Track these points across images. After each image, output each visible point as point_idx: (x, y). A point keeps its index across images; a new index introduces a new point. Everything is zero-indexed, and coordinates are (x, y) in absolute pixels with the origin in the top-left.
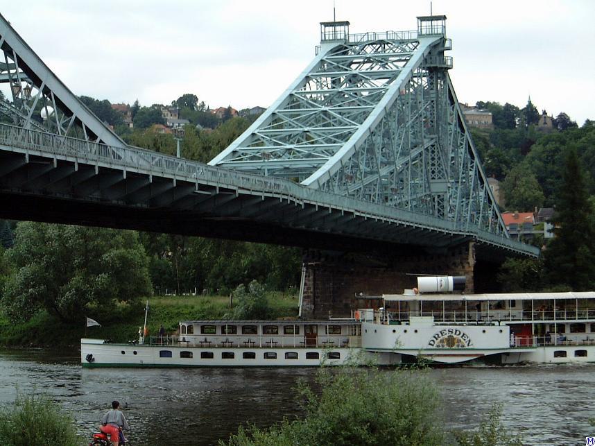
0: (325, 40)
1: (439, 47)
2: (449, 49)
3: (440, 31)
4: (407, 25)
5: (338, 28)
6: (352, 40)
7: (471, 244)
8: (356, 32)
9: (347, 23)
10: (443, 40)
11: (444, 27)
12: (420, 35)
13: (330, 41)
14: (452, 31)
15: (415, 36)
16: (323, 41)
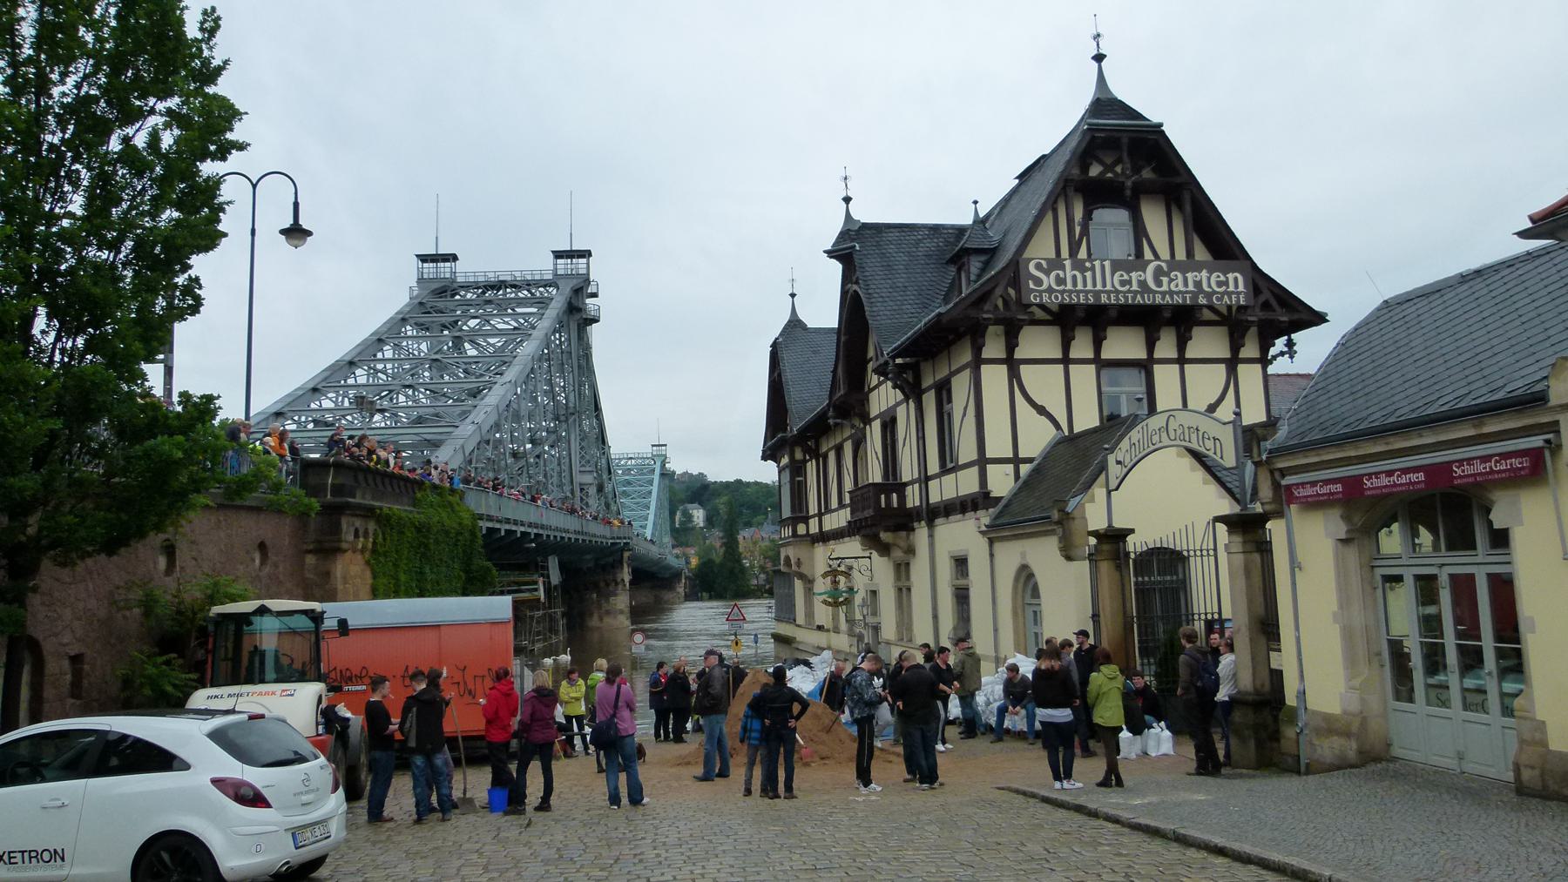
0: (423, 278)
1: (581, 289)
2: (595, 295)
3: (583, 271)
4: (543, 265)
7: (626, 554)
8: (469, 267)
9: (454, 258)
11: (588, 264)
12: (556, 275)
14: (599, 271)
16: (421, 280)
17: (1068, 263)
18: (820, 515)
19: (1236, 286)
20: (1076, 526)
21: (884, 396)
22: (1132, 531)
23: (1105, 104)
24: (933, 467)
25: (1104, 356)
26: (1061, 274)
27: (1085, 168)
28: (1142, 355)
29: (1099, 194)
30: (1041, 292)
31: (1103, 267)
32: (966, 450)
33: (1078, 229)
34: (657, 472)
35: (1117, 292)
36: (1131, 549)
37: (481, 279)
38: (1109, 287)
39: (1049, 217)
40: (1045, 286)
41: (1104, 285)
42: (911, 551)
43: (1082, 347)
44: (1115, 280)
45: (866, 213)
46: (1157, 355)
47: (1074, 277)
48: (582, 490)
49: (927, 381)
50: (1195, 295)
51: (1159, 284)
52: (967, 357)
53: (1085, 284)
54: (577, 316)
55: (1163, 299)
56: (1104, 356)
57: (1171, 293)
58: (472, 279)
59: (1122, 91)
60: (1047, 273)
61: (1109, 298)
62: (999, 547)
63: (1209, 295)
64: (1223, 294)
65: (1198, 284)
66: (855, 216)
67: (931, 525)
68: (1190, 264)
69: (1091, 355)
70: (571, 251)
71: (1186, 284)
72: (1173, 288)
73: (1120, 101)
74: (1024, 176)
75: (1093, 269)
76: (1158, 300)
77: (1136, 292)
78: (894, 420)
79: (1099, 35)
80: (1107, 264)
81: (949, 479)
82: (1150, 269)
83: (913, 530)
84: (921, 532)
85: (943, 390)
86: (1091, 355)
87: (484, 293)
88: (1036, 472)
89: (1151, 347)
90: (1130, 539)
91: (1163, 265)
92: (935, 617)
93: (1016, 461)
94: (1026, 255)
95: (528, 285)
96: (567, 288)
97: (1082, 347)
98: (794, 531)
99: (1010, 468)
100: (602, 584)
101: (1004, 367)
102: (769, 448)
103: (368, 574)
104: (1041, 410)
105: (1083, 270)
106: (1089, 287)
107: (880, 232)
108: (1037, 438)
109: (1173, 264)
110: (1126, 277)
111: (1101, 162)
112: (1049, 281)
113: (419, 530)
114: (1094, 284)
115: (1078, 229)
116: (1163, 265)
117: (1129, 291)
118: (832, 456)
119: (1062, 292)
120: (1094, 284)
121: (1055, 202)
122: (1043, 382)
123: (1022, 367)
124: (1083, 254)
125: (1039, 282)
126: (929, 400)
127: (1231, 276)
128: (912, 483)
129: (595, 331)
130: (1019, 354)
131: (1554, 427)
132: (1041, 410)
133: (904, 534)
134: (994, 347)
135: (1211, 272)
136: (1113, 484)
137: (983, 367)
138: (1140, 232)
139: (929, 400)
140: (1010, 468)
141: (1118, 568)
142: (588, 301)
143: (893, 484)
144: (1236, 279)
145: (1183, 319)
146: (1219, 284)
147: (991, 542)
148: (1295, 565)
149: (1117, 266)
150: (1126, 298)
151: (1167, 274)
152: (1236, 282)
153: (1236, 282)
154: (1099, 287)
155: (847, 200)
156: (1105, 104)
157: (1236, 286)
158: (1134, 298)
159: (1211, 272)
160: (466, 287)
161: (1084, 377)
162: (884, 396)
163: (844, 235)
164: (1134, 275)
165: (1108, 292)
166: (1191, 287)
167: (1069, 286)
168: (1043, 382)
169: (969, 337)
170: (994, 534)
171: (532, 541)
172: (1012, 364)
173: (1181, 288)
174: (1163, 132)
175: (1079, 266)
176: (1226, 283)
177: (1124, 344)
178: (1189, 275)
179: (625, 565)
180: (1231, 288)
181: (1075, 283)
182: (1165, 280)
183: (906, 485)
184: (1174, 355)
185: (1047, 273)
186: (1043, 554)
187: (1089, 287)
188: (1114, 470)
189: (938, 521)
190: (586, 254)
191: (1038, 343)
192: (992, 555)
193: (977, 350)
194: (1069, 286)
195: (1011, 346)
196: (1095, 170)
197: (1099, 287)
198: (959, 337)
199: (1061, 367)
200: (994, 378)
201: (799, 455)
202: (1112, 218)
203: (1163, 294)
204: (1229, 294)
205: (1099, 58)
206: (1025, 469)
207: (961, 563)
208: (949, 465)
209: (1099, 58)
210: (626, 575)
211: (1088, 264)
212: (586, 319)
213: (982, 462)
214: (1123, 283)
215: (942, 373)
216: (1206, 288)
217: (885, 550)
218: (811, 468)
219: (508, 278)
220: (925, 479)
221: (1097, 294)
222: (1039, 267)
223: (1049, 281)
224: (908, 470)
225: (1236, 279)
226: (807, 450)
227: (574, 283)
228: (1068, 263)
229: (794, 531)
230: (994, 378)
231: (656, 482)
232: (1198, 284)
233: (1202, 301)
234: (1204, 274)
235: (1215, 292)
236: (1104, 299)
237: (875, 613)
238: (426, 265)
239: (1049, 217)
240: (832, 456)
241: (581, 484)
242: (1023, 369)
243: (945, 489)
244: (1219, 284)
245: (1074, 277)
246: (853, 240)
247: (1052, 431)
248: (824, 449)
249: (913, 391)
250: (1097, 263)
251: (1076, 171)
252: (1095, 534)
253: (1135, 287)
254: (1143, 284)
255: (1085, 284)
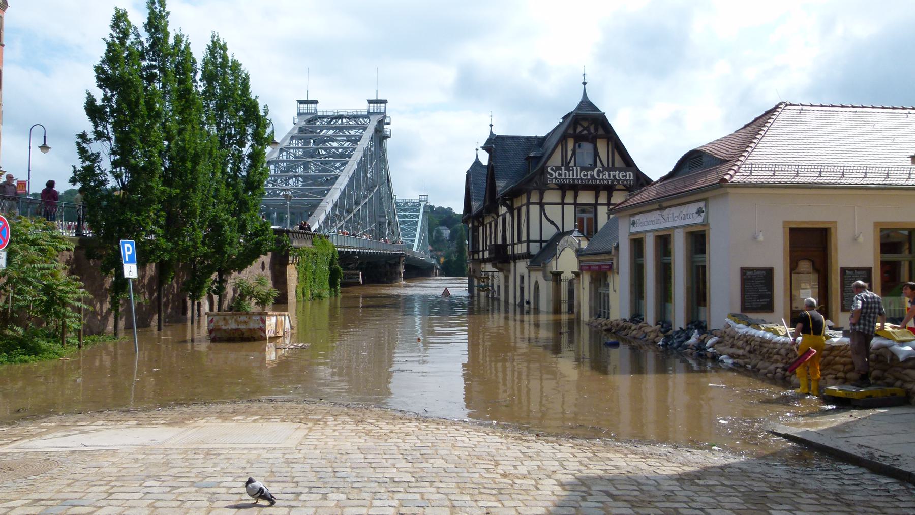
2: (388, 123)
3: (383, 111)
4: (360, 106)
5: (310, 105)
6: (319, 114)
8: (323, 108)
9: (316, 102)
10: (385, 117)
11: (385, 107)
12: (368, 113)
13: (304, 114)
14: (391, 110)
15: (366, 114)
16: (299, 114)
17: (563, 168)
18: (483, 251)
19: (630, 177)
20: (549, 269)
21: (503, 210)
22: (563, 272)
23: (586, 103)
24: (516, 241)
25: (578, 202)
26: (560, 172)
27: (575, 130)
28: (593, 202)
29: (579, 139)
30: (552, 179)
31: (577, 170)
32: (524, 238)
33: (570, 153)
34: (422, 210)
35: (582, 179)
36: (562, 278)
37: (330, 114)
38: (579, 177)
39: (559, 148)
40: (554, 177)
41: (577, 176)
42: (509, 271)
43: (569, 199)
44: (581, 175)
45: (499, 131)
46: (599, 202)
47: (565, 174)
48: (380, 225)
49: (515, 206)
50: (613, 181)
51: (599, 176)
52: (525, 201)
53: (569, 176)
54: (380, 134)
55: (600, 182)
56: (578, 202)
57: (603, 180)
58: (325, 114)
59: (592, 98)
60: (555, 172)
61: (579, 182)
62: (532, 274)
63: (618, 181)
64: (624, 180)
65: (614, 176)
66: (494, 133)
67: (515, 263)
68: (611, 168)
69: (572, 201)
70: (377, 100)
71: (609, 176)
72: (604, 178)
73: (591, 103)
74: (565, 118)
75: (573, 170)
76: (598, 182)
77: (589, 179)
78: (506, 218)
79: (584, 75)
80: (579, 168)
81: (520, 245)
82: (596, 170)
83: (510, 263)
84: (512, 264)
85: (519, 210)
86: (572, 201)
87: (331, 121)
88: (546, 246)
89: (597, 198)
90: (562, 275)
91: (601, 169)
92: (515, 298)
93: (541, 241)
94: (547, 165)
95: (355, 117)
96: (374, 121)
97: (569, 199)
98: (473, 257)
99: (538, 244)
100: (389, 274)
101: (538, 207)
102: (465, 219)
103: (296, 273)
104: (552, 222)
105: (569, 171)
106: (571, 177)
107: (504, 140)
108: (549, 232)
109: (605, 169)
110: (586, 173)
111: (582, 126)
112: (555, 175)
113: (313, 254)
114: (573, 176)
115: (570, 153)
116: (601, 169)
117: (587, 179)
118: (488, 226)
119: (560, 179)
120: (573, 176)
121: (562, 141)
122: (553, 212)
123: (546, 206)
124: (572, 164)
125: (551, 175)
126: (516, 213)
127: (628, 173)
128: (509, 245)
129: (388, 143)
130: (544, 201)
131: (612, 260)
132: (552, 222)
133: (506, 264)
134: (535, 198)
135: (620, 172)
136: (558, 256)
137: (530, 206)
138: (596, 154)
139: (516, 213)
140: (538, 244)
141: (557, 284)
142: (385, 126)
143: (504, 245)
144: (630, 174)
145: (610, 189)
146: (623, 176)
147: (529, 272)
148: (583, 288)
149: (583, 169)
150: (585, 182)
151: (602, 173)
152: (630, 175)
153: (630, 175)
154: (575, 177)
155: (491, 125)
156: (586, 103)
157: (630, 177)
158: (588, 182)
159: (620, 172)
160: (323, 117)
161: (570, 211)
162: (503, 210)
163: (489, 141)
164: (589, 173)
165: (578, 179)
166: (611, 178)
167: (563, 177)
168: (553, 212)
169: (525, 194)
170: (530, 268)
171: (356, 255)
172: (542, 206)
173: (607, 178)
174: (605, 116)
175: (568, 169)
176: (626, 176)
177: (586, 198)
178: (611, 173)
179: (401, 265)
180: (628, 178)
181: (565, 176)
182: (601, 175)
183: (508, 245)
184: (606, 202)
185: (555, 172)
186: (538, 276)
187: (571, 177)
188: (558, 252)
189: (517, 261)
190: (385, 102)
191: (552, 196)
192: (529, 276)
193: (528, 199)
194: (563, 177)
195: (541, 198)
196: (579, 129)
197: (575, 177)
198: (524, 193)
199: (561, 206)
200: (535, 210)
201: (476, 224)
202: (587, 147)
203: (600, 180)
204: (627, 180)
205: (585, 84)
206: (544, 244)
207: (522, 278)
208: (520, 241)
209: (585, 84)
210: (402, 270)
211: (571, 168)
212: (384, 137)
213: (528, 241)
214: (584, 176)
215: (519, 205)
216: (617, 178)
217: (501, 270)
218: (481, 229)
219: (344, 114)
220: (513, 244)
221: (574, 180)
222: (552, 169)
223: (555, 175)
224: (509, 241)
225: (630, 174)
226: (479, 222)
227: (379, 117)
228: (563, 168)
229: (473, 257)
230: (535, 210)
231: (421, 217)
232: (614, 176)
233: (615, 183)
234: (617, 172)
235: (621, 180)
236: (576, 182)
237: (499, 295)
238: (302, 105)
239: (559, 148)
240: (488, 226)
241: (379, 222)
242: (546, 206)
243: (521, 249)
244: (623, 176)
245: (565, 174)
246: (492, 143)
247: (555, 230)
248: (486, 223)
249: (511, 209)
250: (575, 168)
251: (571, 131)
252: (551, 272)
253: (589, 177)
254: (592, 176)
255: (569, 176)
